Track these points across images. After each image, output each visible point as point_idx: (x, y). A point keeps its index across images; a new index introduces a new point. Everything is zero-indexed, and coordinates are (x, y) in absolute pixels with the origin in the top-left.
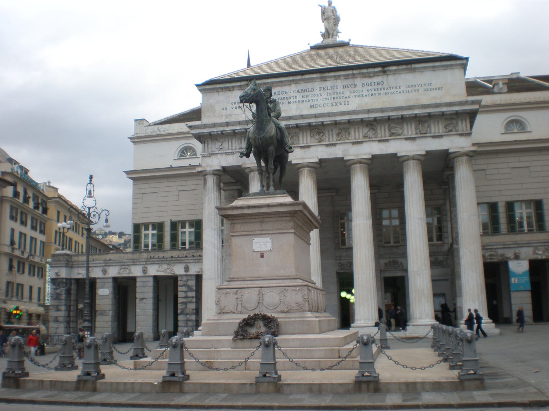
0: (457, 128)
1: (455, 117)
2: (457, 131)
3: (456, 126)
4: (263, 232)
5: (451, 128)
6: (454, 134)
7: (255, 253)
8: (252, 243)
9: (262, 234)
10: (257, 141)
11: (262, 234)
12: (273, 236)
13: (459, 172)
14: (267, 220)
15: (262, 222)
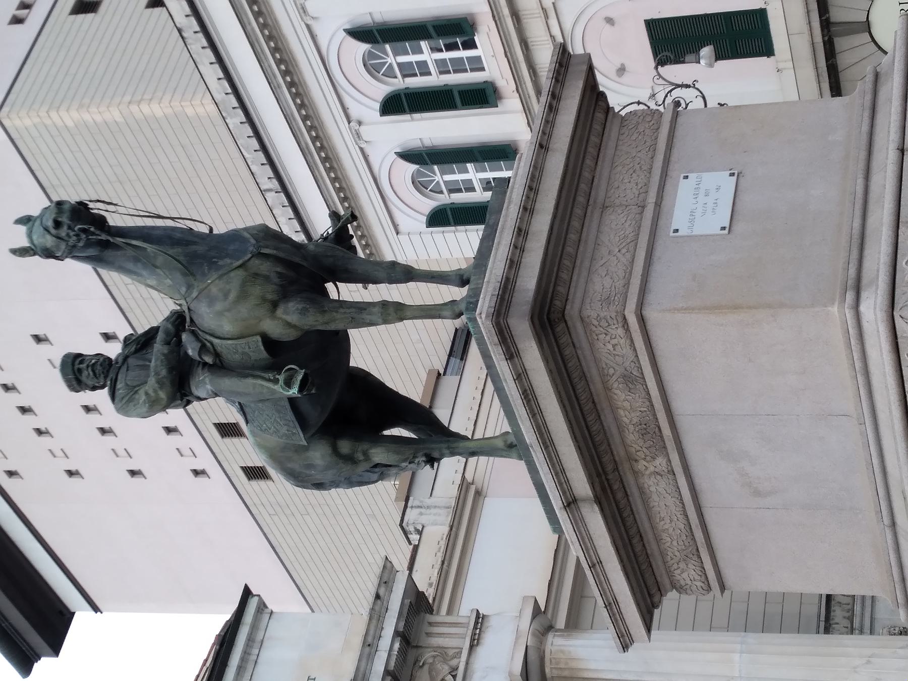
0: (451, 652)
1: (412, 654)
2: (458, 654)
3: (443, 653)
4: (652, 198)
5: (446, 669)
6: (467, 663)
7: (739, 227)
8: (690, 237)
9: (658, 204)
10: (264, 267)
11: (658, 204)
12: (672, 173)
13: (592, 666)
14: (602, 194)
15: (604, 207)
